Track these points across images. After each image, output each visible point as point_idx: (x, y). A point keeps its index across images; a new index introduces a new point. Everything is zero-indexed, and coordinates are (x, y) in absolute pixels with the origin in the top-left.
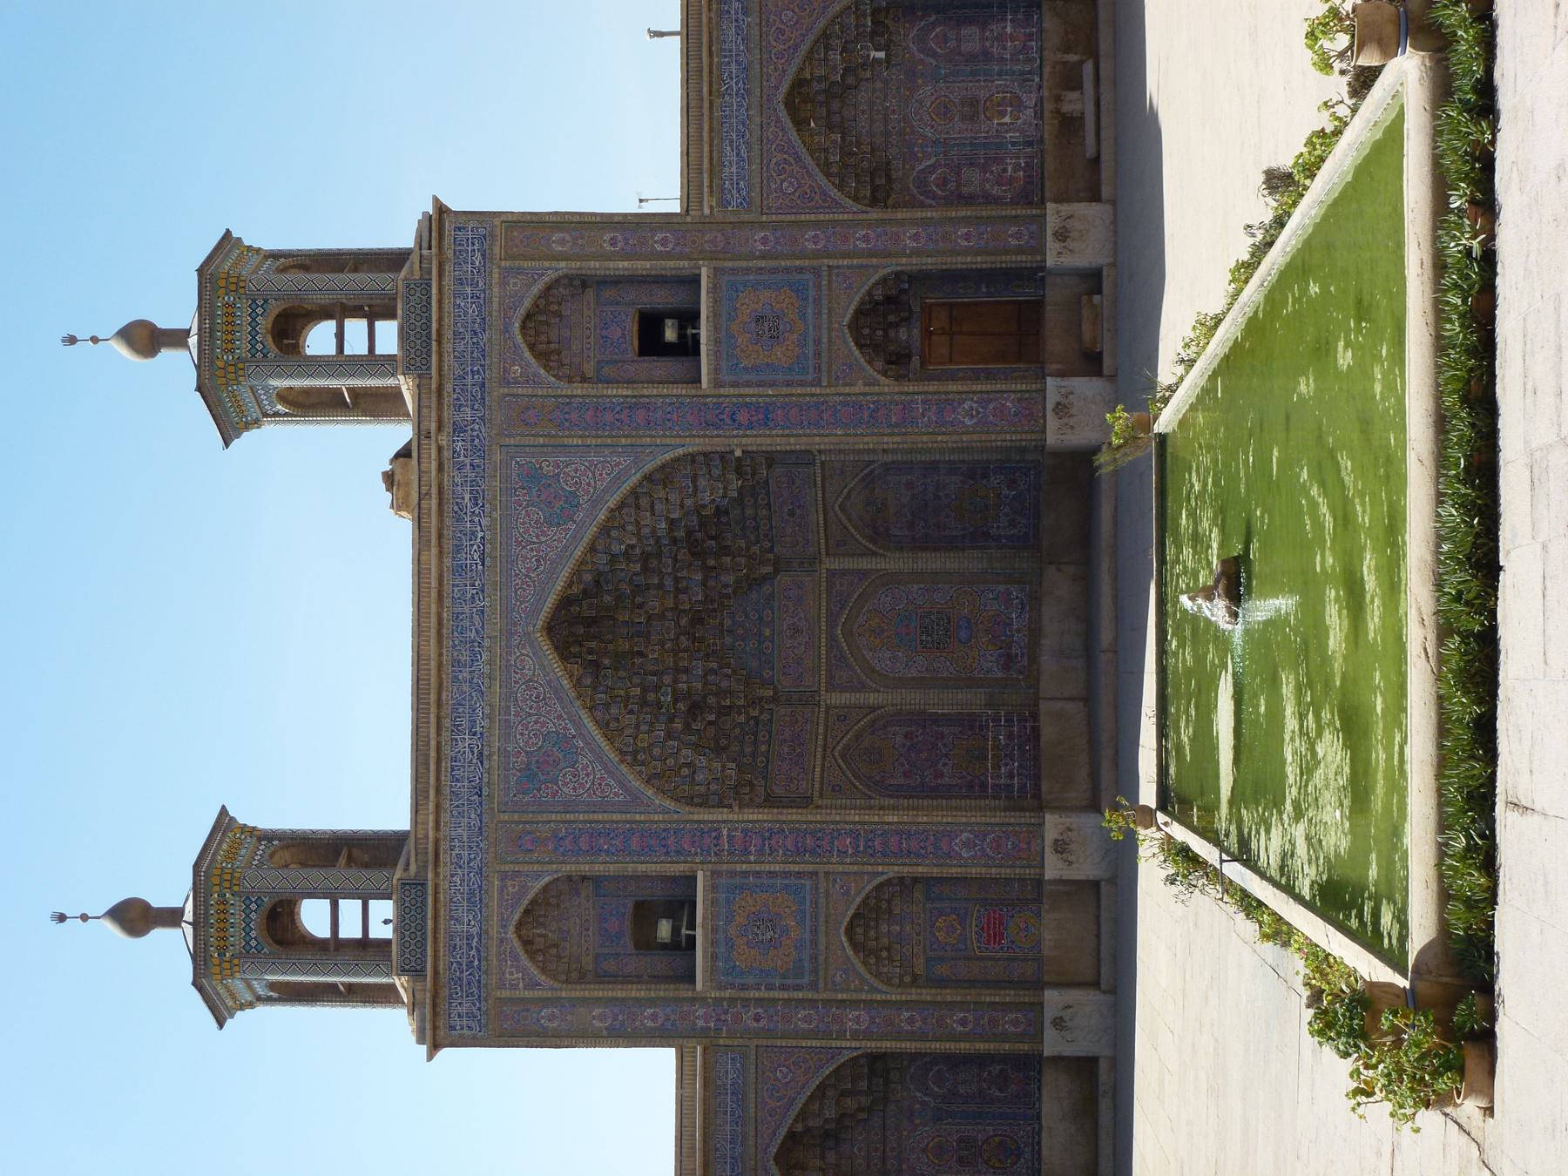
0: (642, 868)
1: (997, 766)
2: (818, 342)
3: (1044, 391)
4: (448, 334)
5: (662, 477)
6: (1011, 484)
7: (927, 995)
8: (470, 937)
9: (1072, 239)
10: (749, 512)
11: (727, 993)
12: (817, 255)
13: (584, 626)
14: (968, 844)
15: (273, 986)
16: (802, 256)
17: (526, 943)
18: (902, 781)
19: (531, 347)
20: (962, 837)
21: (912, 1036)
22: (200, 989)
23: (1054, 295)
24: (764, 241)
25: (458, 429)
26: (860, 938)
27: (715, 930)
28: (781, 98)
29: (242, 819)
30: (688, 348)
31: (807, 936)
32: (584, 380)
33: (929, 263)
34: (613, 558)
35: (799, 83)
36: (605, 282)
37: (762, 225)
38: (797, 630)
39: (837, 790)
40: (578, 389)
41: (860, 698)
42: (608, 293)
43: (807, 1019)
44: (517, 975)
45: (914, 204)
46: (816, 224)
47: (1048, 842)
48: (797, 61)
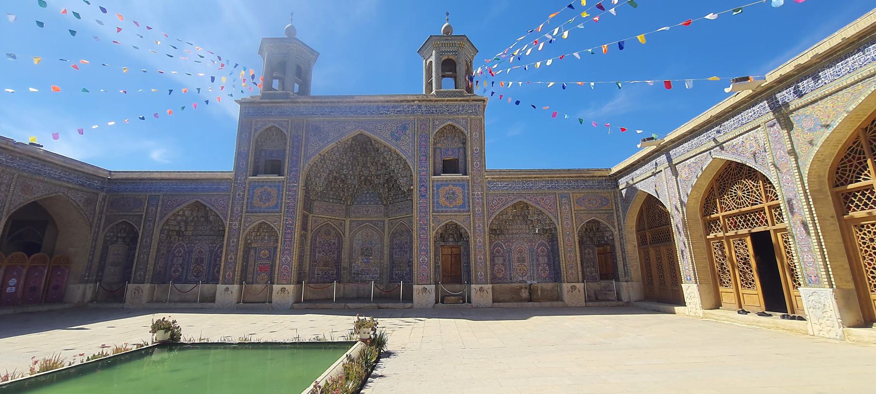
1: (322, 270)
5: (406, 167)
7: (241, 247)
9: (480, 292)
12: (474, 211)
13: (363, 147)
14: (286, 259)
16: (474, 207)
17: (270, 129)
20: (289, 259)
24: (478, 195)
26: (263, 226)
32: (435, 144)
33: (472, 246)
34: (382, 153)
36: (465, 149)
37: (482, 194)
40: (431, 140)
41: (347, 229)
45: (491, 242)
46: (483, 210)
48: (534, 205)
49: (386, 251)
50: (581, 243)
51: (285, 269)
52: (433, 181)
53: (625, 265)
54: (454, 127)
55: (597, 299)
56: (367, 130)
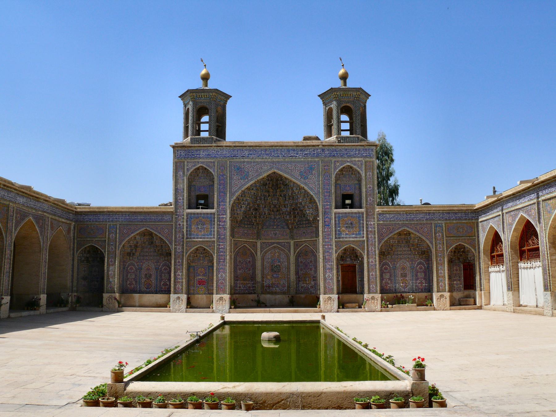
0: (216, 196)
1: (242, 284)
2: (346, 238)
3: (333, 294)
4: (346, 147)
5: (312, 201)
6: (312, 287)
8: (199, 155)
10: (304, 222)
11: (185, 217)
14: (222, 275)
15: (188, 109)
16: (367, 234)
17: (198, 169)
18: (238, 260)
19: (344, 168)
21: (175, 262)
22: (187, 91)
23: (359, 296)
24: (371, 225)
25: (323, 150)
27: (201, 214)
28: (406, 228)
29: (229, 101)
30: (344, 206)
31: (200, 237)
34: (292, 189)
35: (409, 233)
38: (275, 234)
39: (235, 244)
41: (259, 250)
42: (357, 186)
43: (179, 237)
44: (190, 167)
46: (375, 238)
47: (222, 296)
49: (293, 268)
50: (450, 261)
51: (222, 283)
52: (335, 214)
53: (480, 279)
54: (351, 167)
55: (460, 305)
56: (279, 169)
